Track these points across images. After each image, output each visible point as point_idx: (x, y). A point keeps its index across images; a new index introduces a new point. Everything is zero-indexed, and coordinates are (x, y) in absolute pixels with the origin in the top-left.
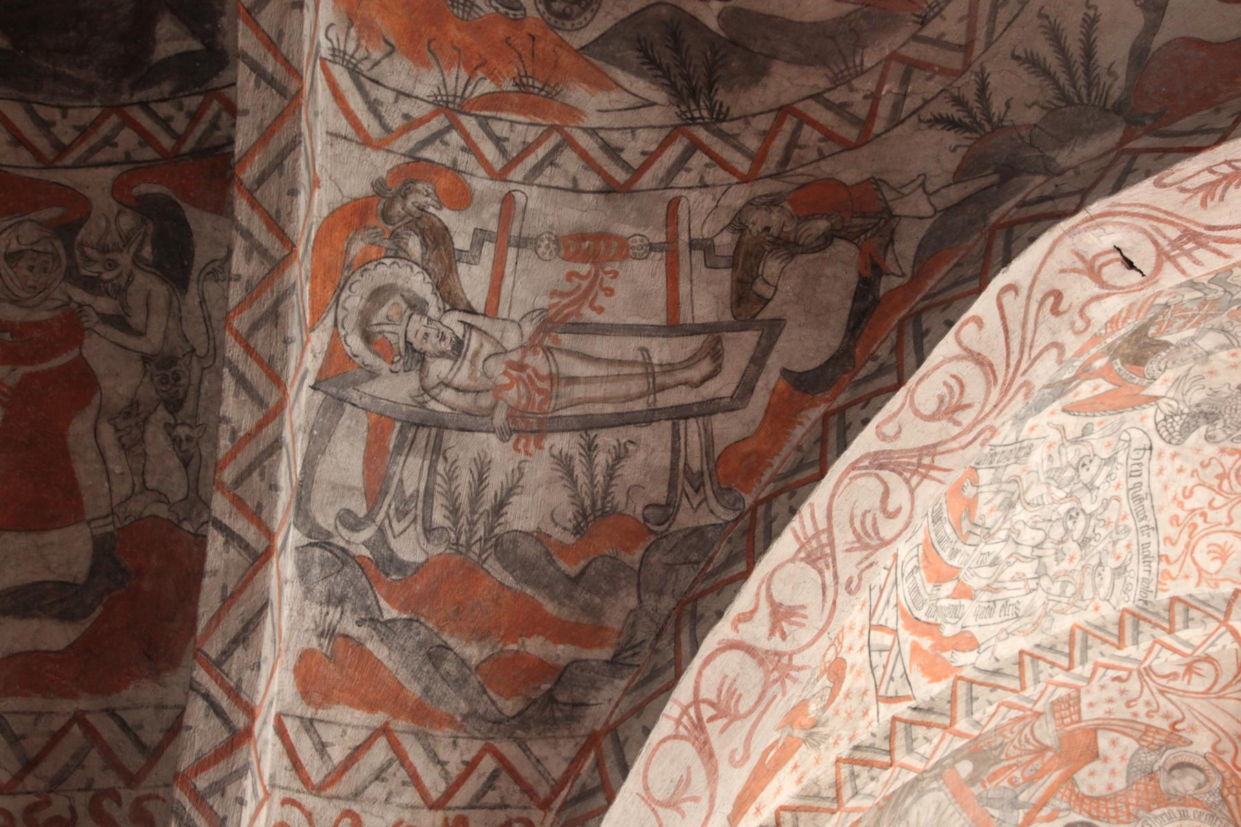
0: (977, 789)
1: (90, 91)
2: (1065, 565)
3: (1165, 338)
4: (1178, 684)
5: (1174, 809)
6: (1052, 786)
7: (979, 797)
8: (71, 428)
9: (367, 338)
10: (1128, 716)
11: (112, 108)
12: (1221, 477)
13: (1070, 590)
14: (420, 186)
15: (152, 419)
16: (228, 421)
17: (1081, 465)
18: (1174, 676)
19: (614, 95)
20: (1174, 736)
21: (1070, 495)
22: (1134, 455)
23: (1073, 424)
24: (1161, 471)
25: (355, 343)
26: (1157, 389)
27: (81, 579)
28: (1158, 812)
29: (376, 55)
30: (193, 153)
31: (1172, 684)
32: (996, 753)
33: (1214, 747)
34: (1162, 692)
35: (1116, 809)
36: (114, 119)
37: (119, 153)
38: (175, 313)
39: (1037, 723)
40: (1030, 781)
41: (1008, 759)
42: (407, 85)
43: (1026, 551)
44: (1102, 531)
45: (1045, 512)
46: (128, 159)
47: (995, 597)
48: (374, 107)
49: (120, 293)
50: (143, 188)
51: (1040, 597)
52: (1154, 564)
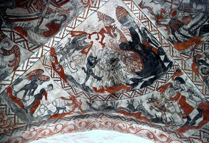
1: (164, 74)
8: (186, 102)
9: (204, 74)
11: (166, 74)
14: (196, 58)
15: (192, 96)
16: (200, 89)
19: (205, 37)
25: (203, 75)
27: (199, 113)
29: (183, 51)
30: (176, 72)
36: (167, 75)
37: (170, 77)
38: (186, 85)
42: (187, 51)
46: (171, 77)
48: (187, 55)
49: (180, 88)
50: (175, 78)
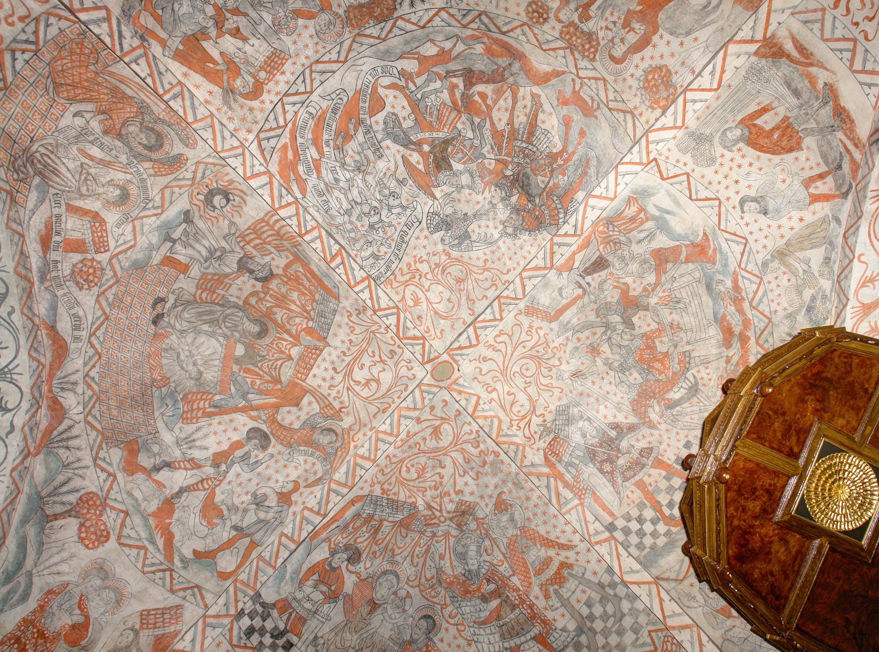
0: (236, 368)
2: (359, 224)
3: (452, 162)
4: (357, 388)
5: (311, 450)
6: (267, 404)
7: (233, 374)
10: (325, 394)
12: (437, 265)
13: (353, 235)
17: (393, 194)
18: (358, 383)
20: (337, 415)
21: (380, 201)
22: (413, 217)
23: (402, 172)
24: (418, 238)
26: (438, 192)
28: (302, 448)
31: (355, 387)
32: (259, 359)
33: (350, 427)
34: (348, 389)
35: (285, 436)
39: (286, 363)
40: (261, 392)
41: (260, 369)
43: (350, 198)
44: (381, 234)
45: (368, 193)
47: (326, 192)
51: (340, 220)
52: (389, 273)
